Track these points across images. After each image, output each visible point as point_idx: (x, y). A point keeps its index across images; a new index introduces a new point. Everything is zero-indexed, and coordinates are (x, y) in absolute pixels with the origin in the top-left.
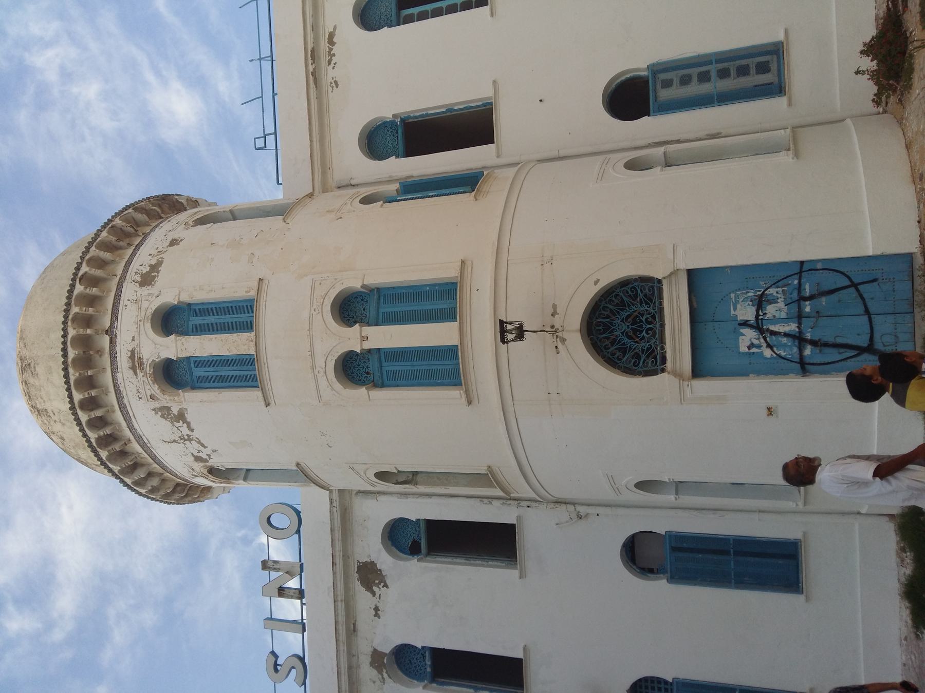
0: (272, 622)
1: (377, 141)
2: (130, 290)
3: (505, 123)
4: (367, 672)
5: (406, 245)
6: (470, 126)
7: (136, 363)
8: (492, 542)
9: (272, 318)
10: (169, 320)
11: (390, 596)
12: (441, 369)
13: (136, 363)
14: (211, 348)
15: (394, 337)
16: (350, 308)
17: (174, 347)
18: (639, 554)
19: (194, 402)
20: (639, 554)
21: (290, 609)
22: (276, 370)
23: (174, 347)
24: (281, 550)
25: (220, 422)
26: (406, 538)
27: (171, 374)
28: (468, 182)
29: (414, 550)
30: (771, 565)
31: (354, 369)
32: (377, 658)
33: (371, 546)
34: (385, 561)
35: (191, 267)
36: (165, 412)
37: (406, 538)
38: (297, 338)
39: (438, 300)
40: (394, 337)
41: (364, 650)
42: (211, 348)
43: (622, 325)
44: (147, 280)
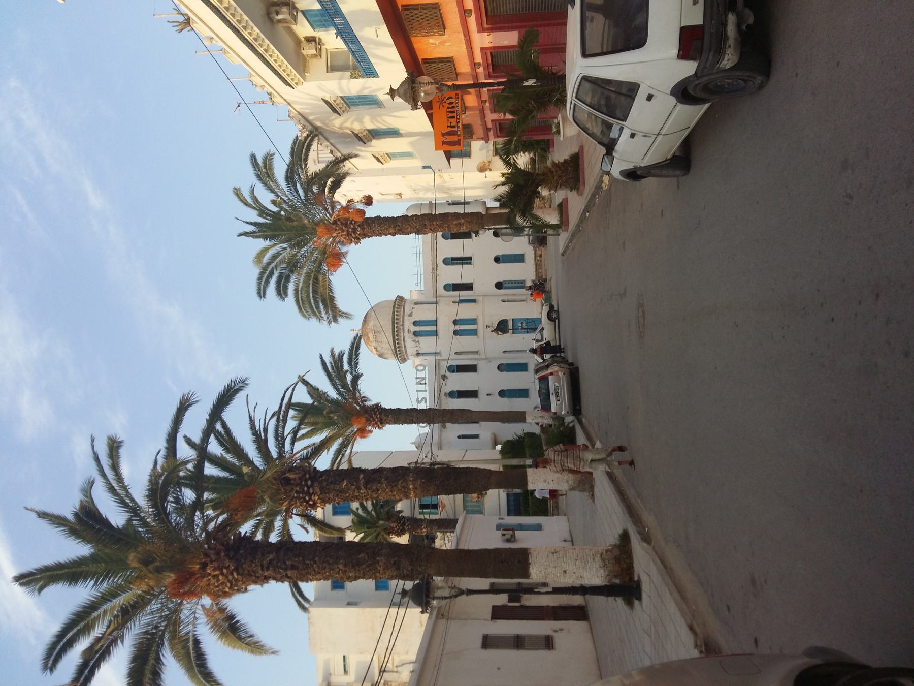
0: (417, 391)
1: (447, 287)
2: (406, 317)
3: (475, 287)
4: (443, 397)
5: (466, 312)
6: (468, 287)
7: (409, 331)
8: (472, 369)
9: (440, 323)
10: (415, 323)
11: (448, 381)
12: (474, 333)
13: (409, 331)
14: (427, 329)
15: (464, 327)
16: (455, 322)
17: (418, 329)
18: (500, 368)
19: (421, 339)
20: (500, 368)
21: (422, 387)
22: (440, 333)
23: (418, 329)
24: (421, 374)
25: (427, 343)
26: (452, 369)
27: (416, 334)
28: (474, 301)
29: (453, 372)
30: (523, 367)
31: (456, 333)
32: (446, 394)
33: (443, 371)
34: (448, 374)
35: (425, 314)
36: (414, 341)
37: (452, 369)
38: (445, 327)
39: (474, 321)
40: (464, 327)
41: (443, 393)
42: (427, 329)
43: (502, 327)
44: (410, 315)
